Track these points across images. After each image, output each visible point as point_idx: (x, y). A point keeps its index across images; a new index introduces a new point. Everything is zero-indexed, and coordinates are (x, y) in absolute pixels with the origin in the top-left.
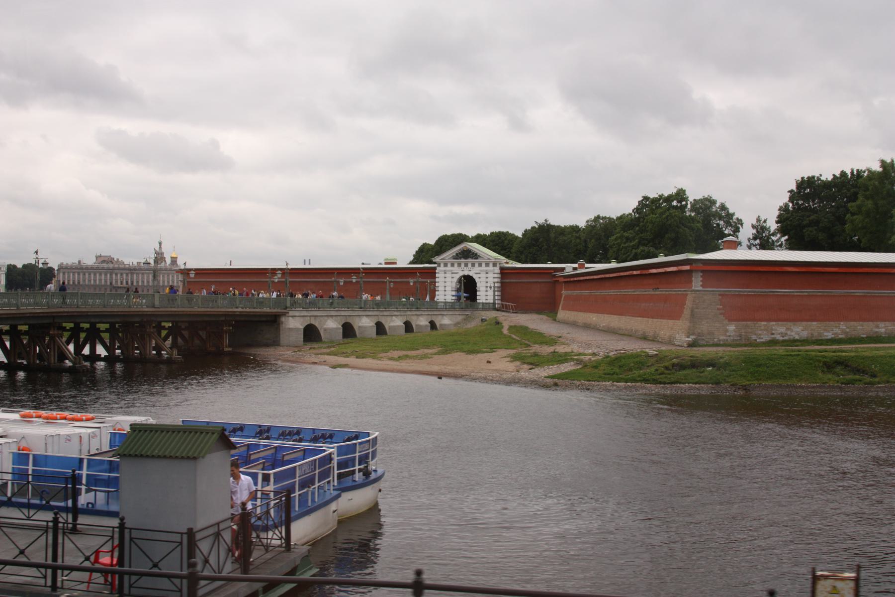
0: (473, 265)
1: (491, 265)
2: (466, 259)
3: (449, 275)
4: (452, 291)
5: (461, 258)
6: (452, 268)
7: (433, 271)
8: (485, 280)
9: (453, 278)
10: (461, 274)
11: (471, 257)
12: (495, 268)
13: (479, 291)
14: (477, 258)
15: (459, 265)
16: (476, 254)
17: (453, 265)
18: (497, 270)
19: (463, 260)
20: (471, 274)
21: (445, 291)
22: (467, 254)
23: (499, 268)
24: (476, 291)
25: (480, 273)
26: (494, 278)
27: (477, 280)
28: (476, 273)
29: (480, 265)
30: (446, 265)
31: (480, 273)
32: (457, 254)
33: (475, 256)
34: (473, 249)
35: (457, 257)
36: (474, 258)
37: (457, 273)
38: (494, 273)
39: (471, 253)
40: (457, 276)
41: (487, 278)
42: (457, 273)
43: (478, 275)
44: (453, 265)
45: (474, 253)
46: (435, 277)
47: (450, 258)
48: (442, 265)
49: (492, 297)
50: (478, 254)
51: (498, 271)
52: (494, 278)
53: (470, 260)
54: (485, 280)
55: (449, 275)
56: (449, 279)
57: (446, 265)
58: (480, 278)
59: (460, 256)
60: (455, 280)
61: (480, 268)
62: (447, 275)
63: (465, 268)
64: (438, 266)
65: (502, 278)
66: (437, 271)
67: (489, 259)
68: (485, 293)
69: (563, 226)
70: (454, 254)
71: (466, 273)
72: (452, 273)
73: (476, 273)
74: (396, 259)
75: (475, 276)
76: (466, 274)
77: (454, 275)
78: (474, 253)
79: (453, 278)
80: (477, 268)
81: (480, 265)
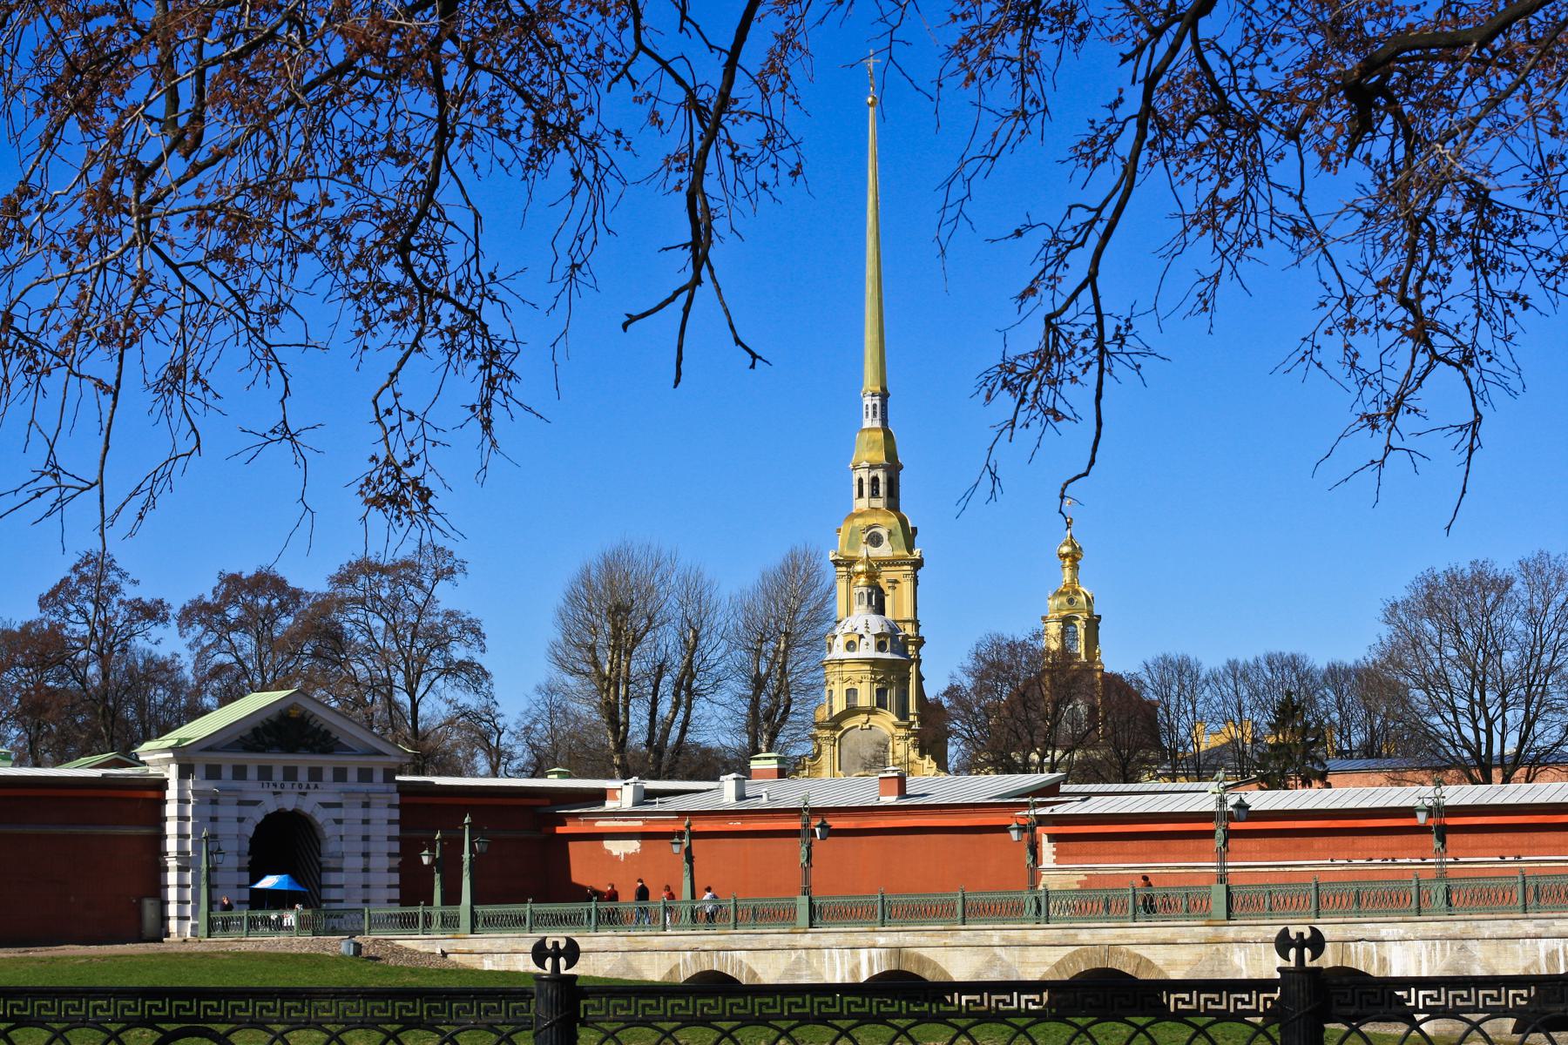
1: (378, 776)
6: (237, 784)
8: (360, 830)
10: (271, 806)
13: (340, 870)
15: (265, 773)
16: (327, 733)
19: (278, 760)
25: (339, 805)
27: (329, 831)
28: (326, 805)
29: (340, 775)
31: (339, 805)
32: (255, 731)
36: (317, 748)
37: (255, 803)
40: (257, 815)
42: (255, 803)
44: (240, 772)
50: (334, 736)
51: (396, 799)
53: (303, 761)
58: (339, 822)
59: (267, 739)
60: (250, 830)
61: (340, 786)
62: (221, 811)
63: (288, 784)
67: (379, 753)
68: (374, 879)
71: (289, 803)
72: (241, 803)
73: (326, 805)
75: (321, 817)
76: (290, 809)
80: (329, 790)
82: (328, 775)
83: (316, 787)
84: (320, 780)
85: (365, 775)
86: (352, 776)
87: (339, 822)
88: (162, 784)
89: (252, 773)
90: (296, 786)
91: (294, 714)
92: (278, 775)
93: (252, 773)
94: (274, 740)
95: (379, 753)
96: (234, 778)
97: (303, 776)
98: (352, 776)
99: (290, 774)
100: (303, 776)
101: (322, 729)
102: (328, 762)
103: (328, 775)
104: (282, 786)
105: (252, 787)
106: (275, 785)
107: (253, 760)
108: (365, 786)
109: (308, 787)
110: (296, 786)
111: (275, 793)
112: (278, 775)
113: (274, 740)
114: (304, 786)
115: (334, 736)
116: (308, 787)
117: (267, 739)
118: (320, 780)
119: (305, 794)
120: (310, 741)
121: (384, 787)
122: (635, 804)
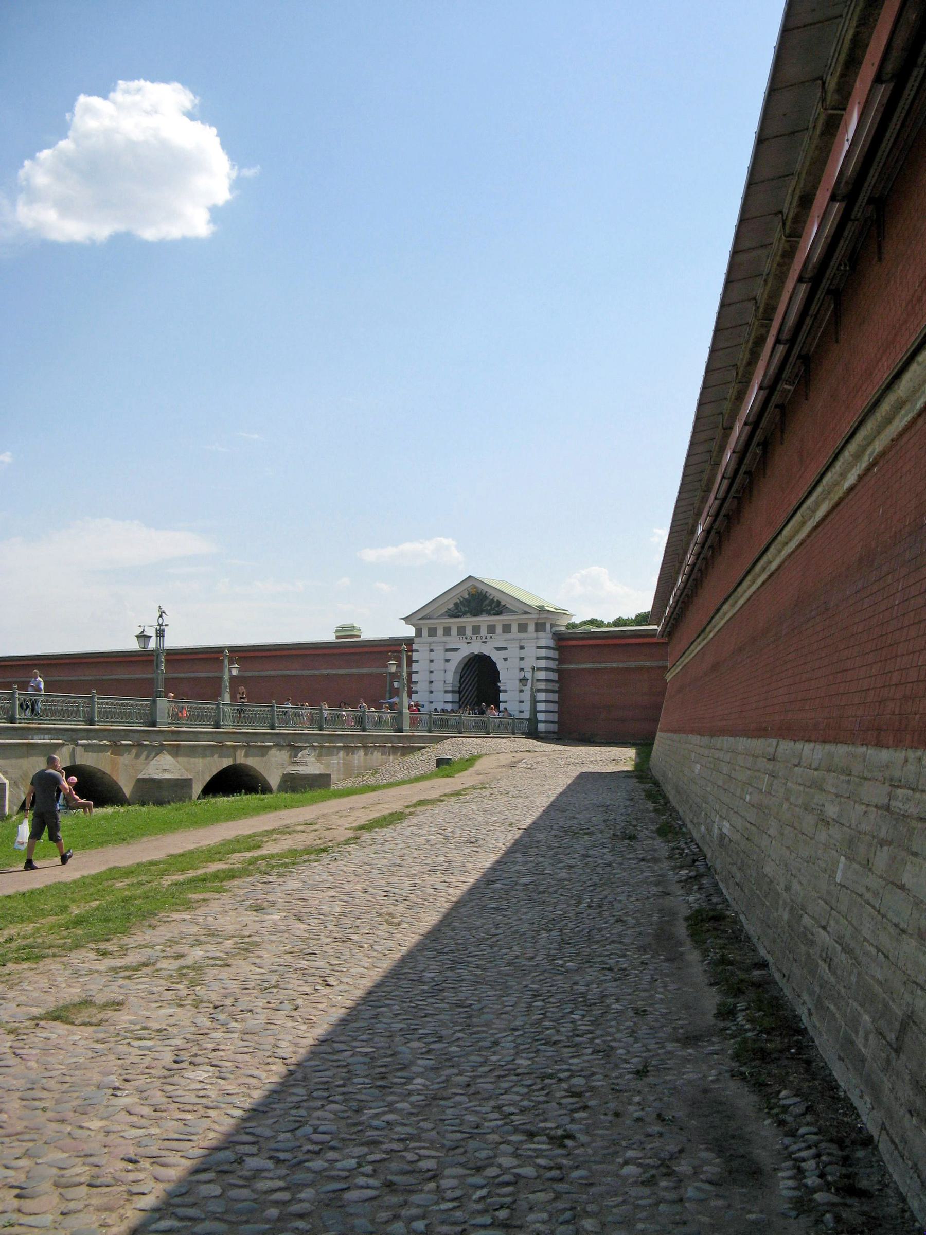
0: (492, 629)
2: (475, 616)
4: (446, 692)
5: (464, 614)
9: (447, 661)
11: (489, 613)
12: (541, 634)
13: (505, 691)
14: (499, 613)
16: (499, 602)
17: (447, 631)
18: (546, 640)
19: (469, 621)
20: (487, 650)
21: (431, 692)
23: (551, 636)
24: (498, 691)
25: (505, 649)
26: (538, 658)
28: (498, 649)
29: (507, 629)
30: (432, 632)
31: (505, 649)
32: (456, 604)
34: (490, 591)
36: (492, 612)
38: (538, 648)
39: (487, 602)
40: (457, 659)
41: (522, 659)
43: (503, 654)
44: (447, 631)
45: (492, 600)
47: (442, 615)
49: (527, 706)
50: (503, 603)
52: (538, 658)
53: (484, 620)
54: (514, 663)
56: (438, 665)
57: (432, 632)
58: (506, 659)
59: (463, 609)
60: (453, 666)
61: (507, 636)
63: (474, 637)
65: (561, 660)
67: (526, 613)
70: (451, 606)
71: (477, 648)
72: (447, 650)
73: (498, 649)
74: (360, 630)
75: (496, 657)
76: (476, 653)
77: (450, 655)
78: (492, 600)
79: (447, 661)
80: (499, 640)
81: (507, 629)
82: (499, 629)
83: (491, 637)
84: (494, 633)
85: (523, 628)
86: (514, 628)
89: (454, 631)
90: (479, 638)
92: (469, 632)
93: (454, 631)
94: (467, 609)
95: (526, 613)
96: (519, 632)
97: (484, 631)
98: (514, 628)
100: (484, 631)
101: (495, 599)
103: (499, 629)
104: (471, 638)
105: (453, 641)
106: (466, 638)
108: (432, 639)
109: (486, 638)
110: (479, 638)
111: (468, 643)
112: (469, 632)
113: (467, 609)
114: (484, 637)
115: (503, 603)
116: (486, 638)
117: (463, 609)
118: (494, 633)
119: (485, 642)
120: (489, 608)
121: (534, 635)
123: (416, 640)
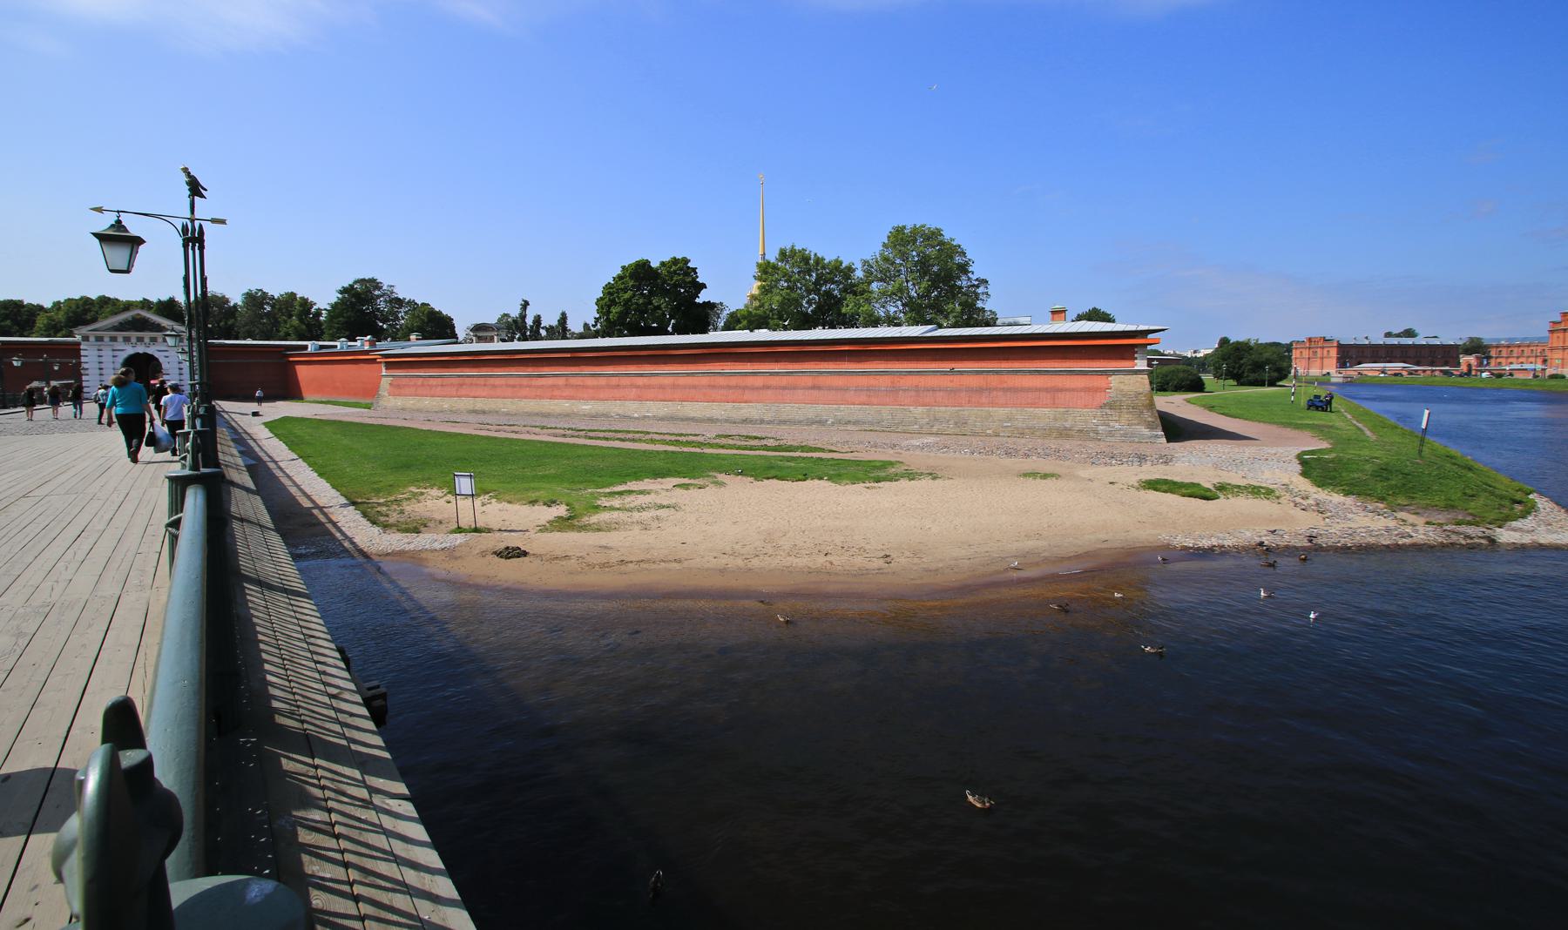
0: (154, 340)
3: (107, 353)
6: (111, 343)
7: (75, 347)
10: (130, 350)
11: (151, 331)
15: (127, 340)
19: (134, 335)
20: (149, 351)
22: (140, 325)
30: (99, 339)
32: (121, 323)
33: (158, 328)
35: (121, 327)
40: (123, 356)
46: (79, 356)
48: (92, 339)
53: (147, 335)
55: (107, 353)
64: (83, 340)
66: (82, 347)
69: (236, 298)
71: (141, 349)
72: (114, 350)
75: (157, 355)
76: (141, 352)
78: (154, 323)
87: (167, 357)
88: (79, 344)
91: (139, 317)
97: (147, 340)
99: (140, 340)
100: (147, 340)
102: (159, 335)
105: (120, 345)
107: (120, 335)
122: (315, 350)
123: (83, 343)
